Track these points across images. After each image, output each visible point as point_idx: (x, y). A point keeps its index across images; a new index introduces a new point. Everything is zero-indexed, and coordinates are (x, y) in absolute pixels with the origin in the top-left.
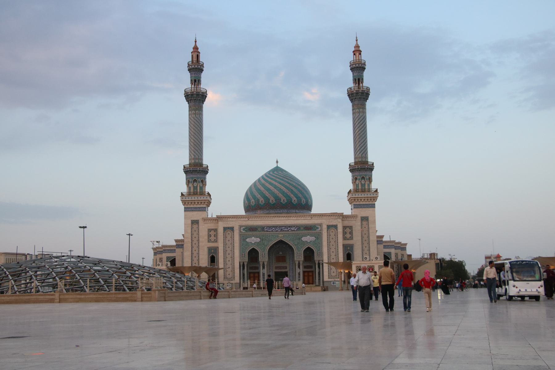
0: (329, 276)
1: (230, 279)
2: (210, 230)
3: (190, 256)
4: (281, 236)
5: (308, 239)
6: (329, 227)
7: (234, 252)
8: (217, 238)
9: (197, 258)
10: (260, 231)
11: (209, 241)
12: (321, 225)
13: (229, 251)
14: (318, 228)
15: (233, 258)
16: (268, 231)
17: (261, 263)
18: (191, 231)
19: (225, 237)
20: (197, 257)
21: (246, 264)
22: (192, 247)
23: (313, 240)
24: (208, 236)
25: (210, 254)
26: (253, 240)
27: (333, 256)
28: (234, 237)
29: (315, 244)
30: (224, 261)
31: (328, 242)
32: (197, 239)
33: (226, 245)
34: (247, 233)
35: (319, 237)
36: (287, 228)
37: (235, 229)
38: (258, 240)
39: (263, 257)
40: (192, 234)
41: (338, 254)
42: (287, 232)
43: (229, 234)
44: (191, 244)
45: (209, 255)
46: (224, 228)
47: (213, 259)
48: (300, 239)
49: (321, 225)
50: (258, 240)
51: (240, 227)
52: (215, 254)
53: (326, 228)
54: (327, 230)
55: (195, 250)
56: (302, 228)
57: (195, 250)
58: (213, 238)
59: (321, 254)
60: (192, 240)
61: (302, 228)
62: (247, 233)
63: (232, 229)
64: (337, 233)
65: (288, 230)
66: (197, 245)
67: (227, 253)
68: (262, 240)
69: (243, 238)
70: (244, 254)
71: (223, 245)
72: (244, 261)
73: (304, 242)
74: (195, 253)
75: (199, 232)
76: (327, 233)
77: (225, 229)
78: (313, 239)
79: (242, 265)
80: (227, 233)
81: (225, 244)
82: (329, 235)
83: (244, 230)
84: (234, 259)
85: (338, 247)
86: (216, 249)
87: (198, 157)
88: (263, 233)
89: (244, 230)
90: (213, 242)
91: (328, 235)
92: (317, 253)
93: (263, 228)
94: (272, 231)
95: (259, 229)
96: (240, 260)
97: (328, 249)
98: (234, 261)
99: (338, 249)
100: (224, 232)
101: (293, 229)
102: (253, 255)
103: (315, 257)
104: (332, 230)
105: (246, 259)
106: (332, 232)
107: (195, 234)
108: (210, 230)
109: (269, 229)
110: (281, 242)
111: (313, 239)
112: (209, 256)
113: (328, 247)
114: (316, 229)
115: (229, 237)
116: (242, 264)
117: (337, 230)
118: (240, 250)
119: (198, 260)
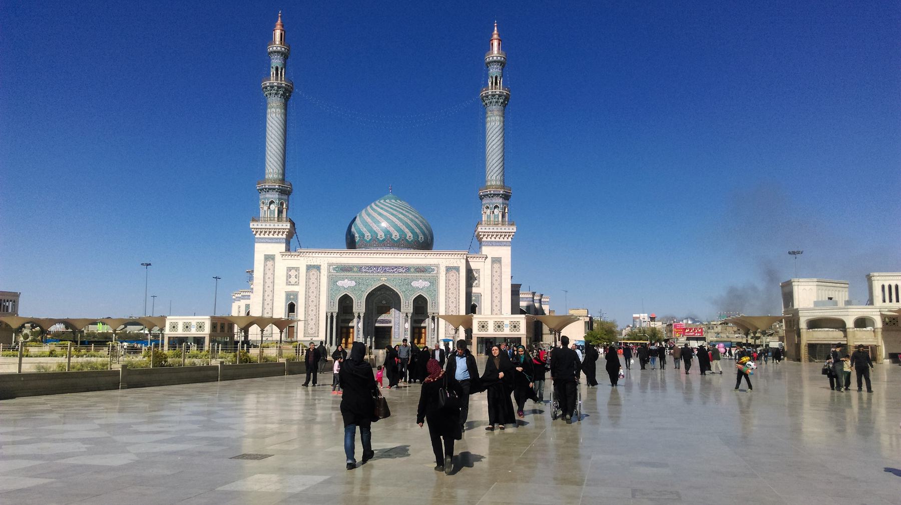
0: (446, 334)
1: (313, 335)
2: (289, 269)
3: (262, 303)
4: (384, 279)
5: (420, 285)
6: (448, 269)
7: (319, 298)
8: (298, 280)
9: (270, 306)
10: (356, 272)
11: (288, 283)
12: (437, 266)
13: (312, 297)
14: (433, 270)
15: (318, 307)
16: (366, 272)
17: (356, 315)
18: (263, 269)
19: (308, 279)
20: (270, 304)
21: (335, 315)
22: (264, 291)
23: (426, 285)
24: (287, 276)
25: (289, 301)
26: (346, 284)
27: (452, 306)
28: (320, 279)
29: (430, 291)
30: (305, 311)
31: (446, 289)
32: (271, 280)
33: (309, 289)
34: (338, 274)
35: (434, 282)
36: (393, 269)
37: (322, 267)
38: (353, 283)
39: (359, 308)
40: (265, 274)
41: (459, 305)
42: (391, 274)
43: (313, 274)
44: (262, 287)
45: (286, 302)
46: (307, 265)
47: (292, 308)
48: (409, 284)
49: (437, 266)
50: (353, 283)
51: (330, 265)
52: (295, 301)
53: (445, 270)
54: (446, 274)
55: (268, 296)
56: (412, 270)
57: (268, 296)
58: (293, 280)
59: (436, 304)
60: (264, 282)
61: (412, 270)
62: (338, 274)
63: (318, 268)
64: (459, 277)
65: (394, 272)
66: (271, 288)
67: (310, 300)
68: (358, 283)
69: (332, 281)
70: (333, 302)
71: (304, 289)
72: (332, 311)
73: (413, 287)
74: (268, 299)
75: (274, 271)
76: (446, 277)
77: (309, 268)
78: (427, 284)
79: (329, 317)
80: (311, 273)
81: (307, 288)
82: (447, 280)
83: (334, 269)
84: (319, 308)
85: (459, 296)
86: (296, 295)
87: (272, 171)
88: (360, 274)
89: (334, 269)
90: (294, 285)
91: (446, 280)
92: (431, 303)
93: (360, 268)
94: (372, 272)
95: (355, 269)
96: (327, 310)
97: (446, 299)
98: (319, 311)
99: (459, 299)
100: (307, 272)
101: (401, 270)
102: (345, 304)
103: (428, 308)
104: (453, 273)
105: (336, 309)
106: (453, 276)
107: (269, 274)
108: (289, 269)
109: (368, 270)
110: (383, 288)
111: (427, 284)
112: (286, 304)
113: (446, 296)
114: (431, 271)
115: (313, 279)
116: (329, 315)
117: (459, 274)
118: (328, 297)
119: (272, 309)
